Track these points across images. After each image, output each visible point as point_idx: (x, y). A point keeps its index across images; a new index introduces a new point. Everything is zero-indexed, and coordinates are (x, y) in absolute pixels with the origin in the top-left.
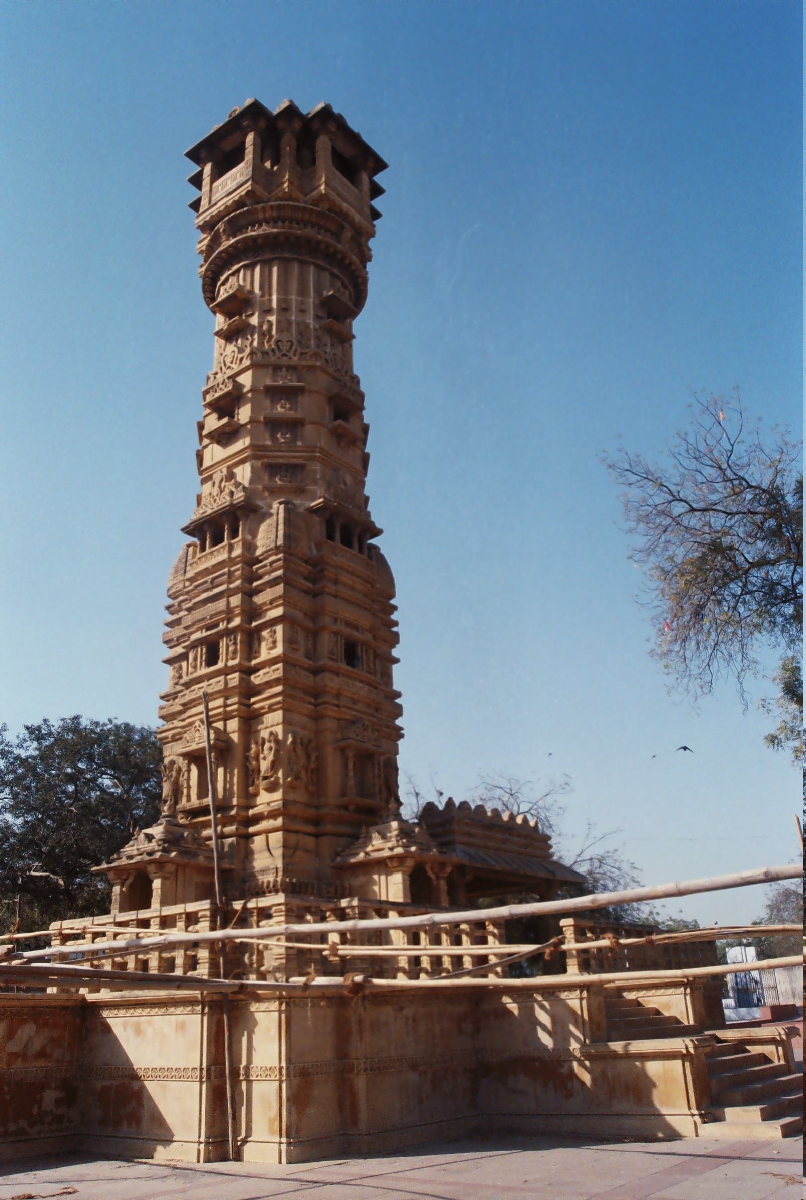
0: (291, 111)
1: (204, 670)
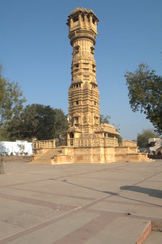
1: (76, 105)
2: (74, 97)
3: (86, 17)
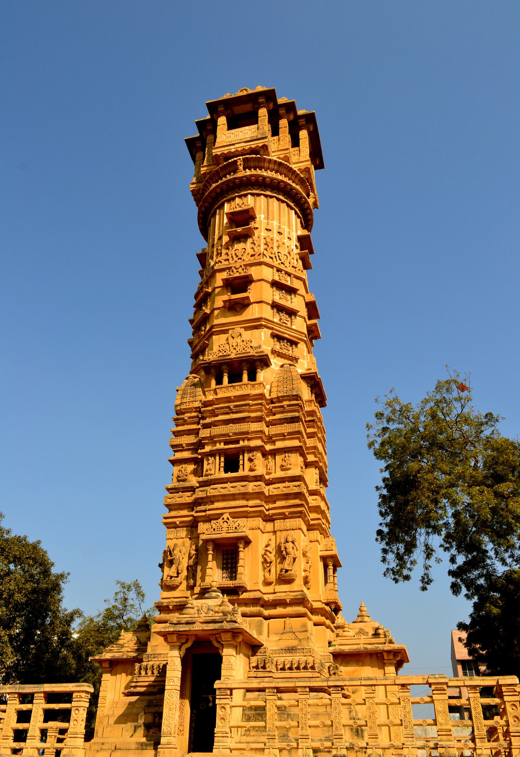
0: (290, 107)
1: (223, 475)
2: (216, 431)
3: (284, 123)
